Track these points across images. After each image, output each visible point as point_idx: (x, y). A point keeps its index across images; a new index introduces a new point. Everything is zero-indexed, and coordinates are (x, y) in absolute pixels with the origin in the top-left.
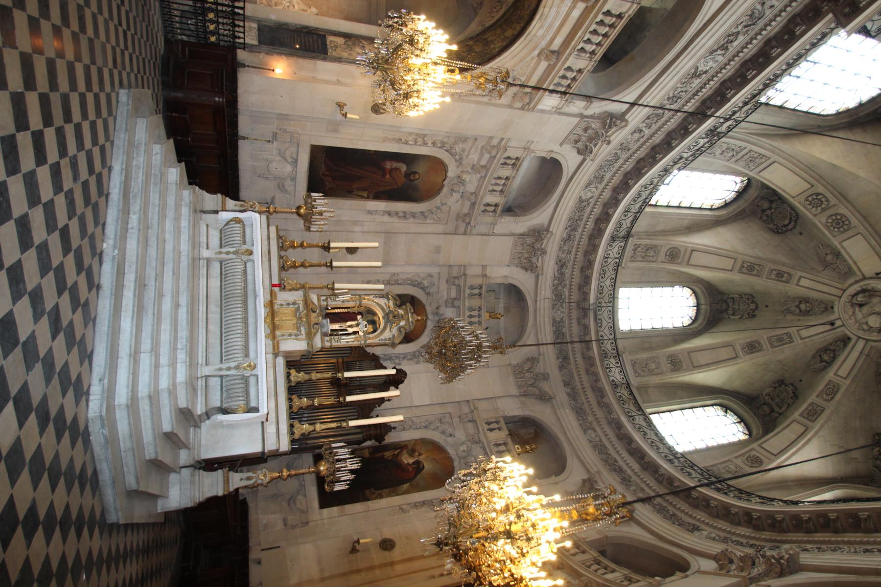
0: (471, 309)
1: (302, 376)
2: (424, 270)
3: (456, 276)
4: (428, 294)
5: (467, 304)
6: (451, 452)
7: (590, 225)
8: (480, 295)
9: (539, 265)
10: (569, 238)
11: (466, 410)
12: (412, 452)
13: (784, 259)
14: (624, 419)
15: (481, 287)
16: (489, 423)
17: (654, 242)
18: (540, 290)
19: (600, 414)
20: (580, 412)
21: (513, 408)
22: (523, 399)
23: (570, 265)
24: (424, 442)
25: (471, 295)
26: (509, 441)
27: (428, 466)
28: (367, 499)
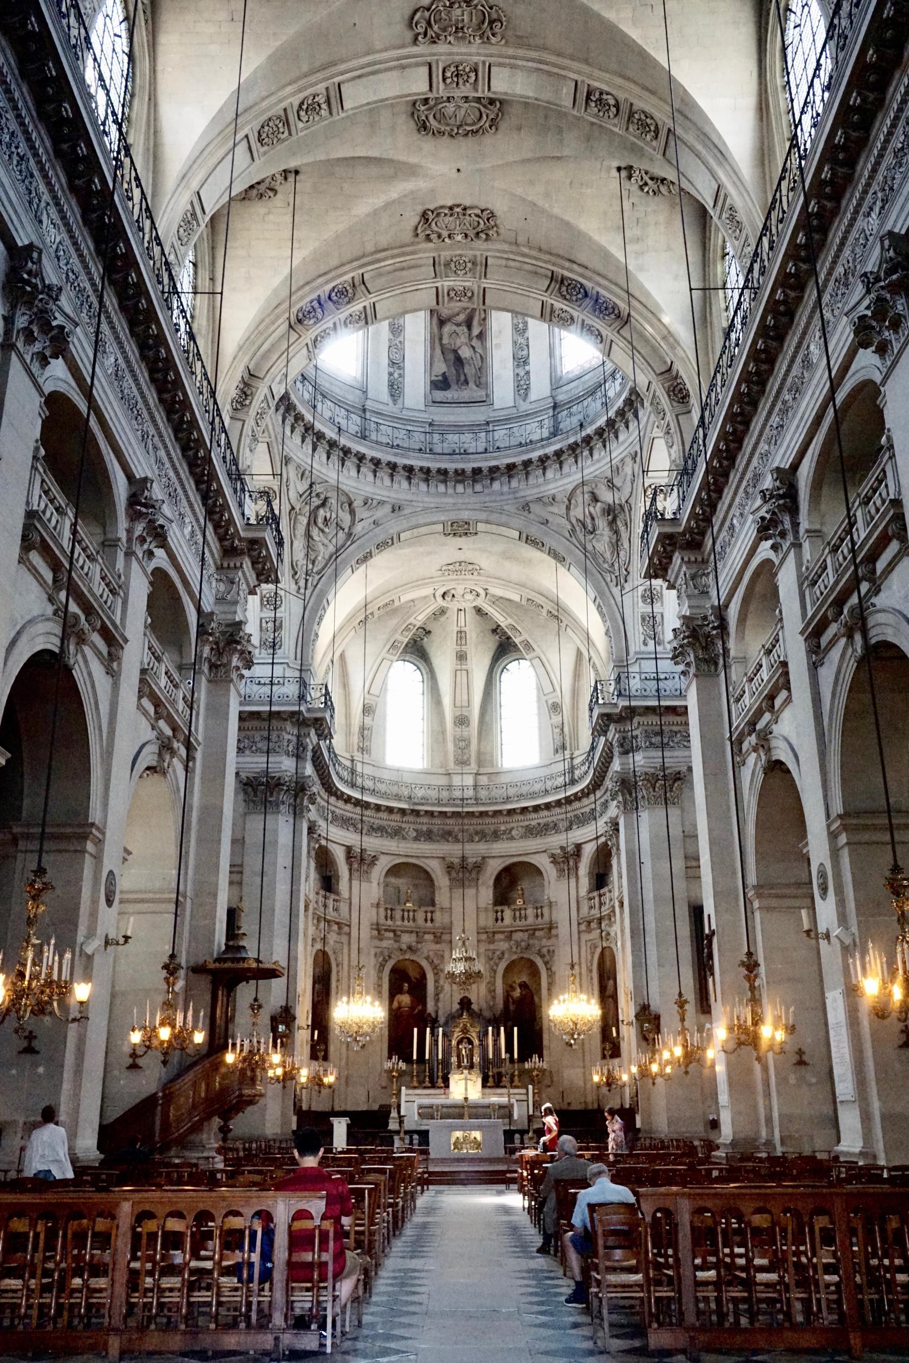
0: (403, 919)
1: (491, 1079)
2: (373, 961)
3: (378, 930)
4: (390, 957)
5: (399, 923)
6: (515, 957)
7: (349, 807)
8: (392, 910)
9: (373, 854)
10: (354, 825)
11: (484, 937)
12: (512, 988)
13: (395, 621)
14: (509, 807)
15: (386, 909)
16: (497, 920)
17: (355, 729)
18: (389, 850)
19: (502, 819)
20: (496, 836)
21: (486, 894)
22: (480, 882)
23: (372, 820)
24: (504, 976)
25: (392, 918)
26: (513, 907)
27: (524, 978)
28: (541, 1029)
